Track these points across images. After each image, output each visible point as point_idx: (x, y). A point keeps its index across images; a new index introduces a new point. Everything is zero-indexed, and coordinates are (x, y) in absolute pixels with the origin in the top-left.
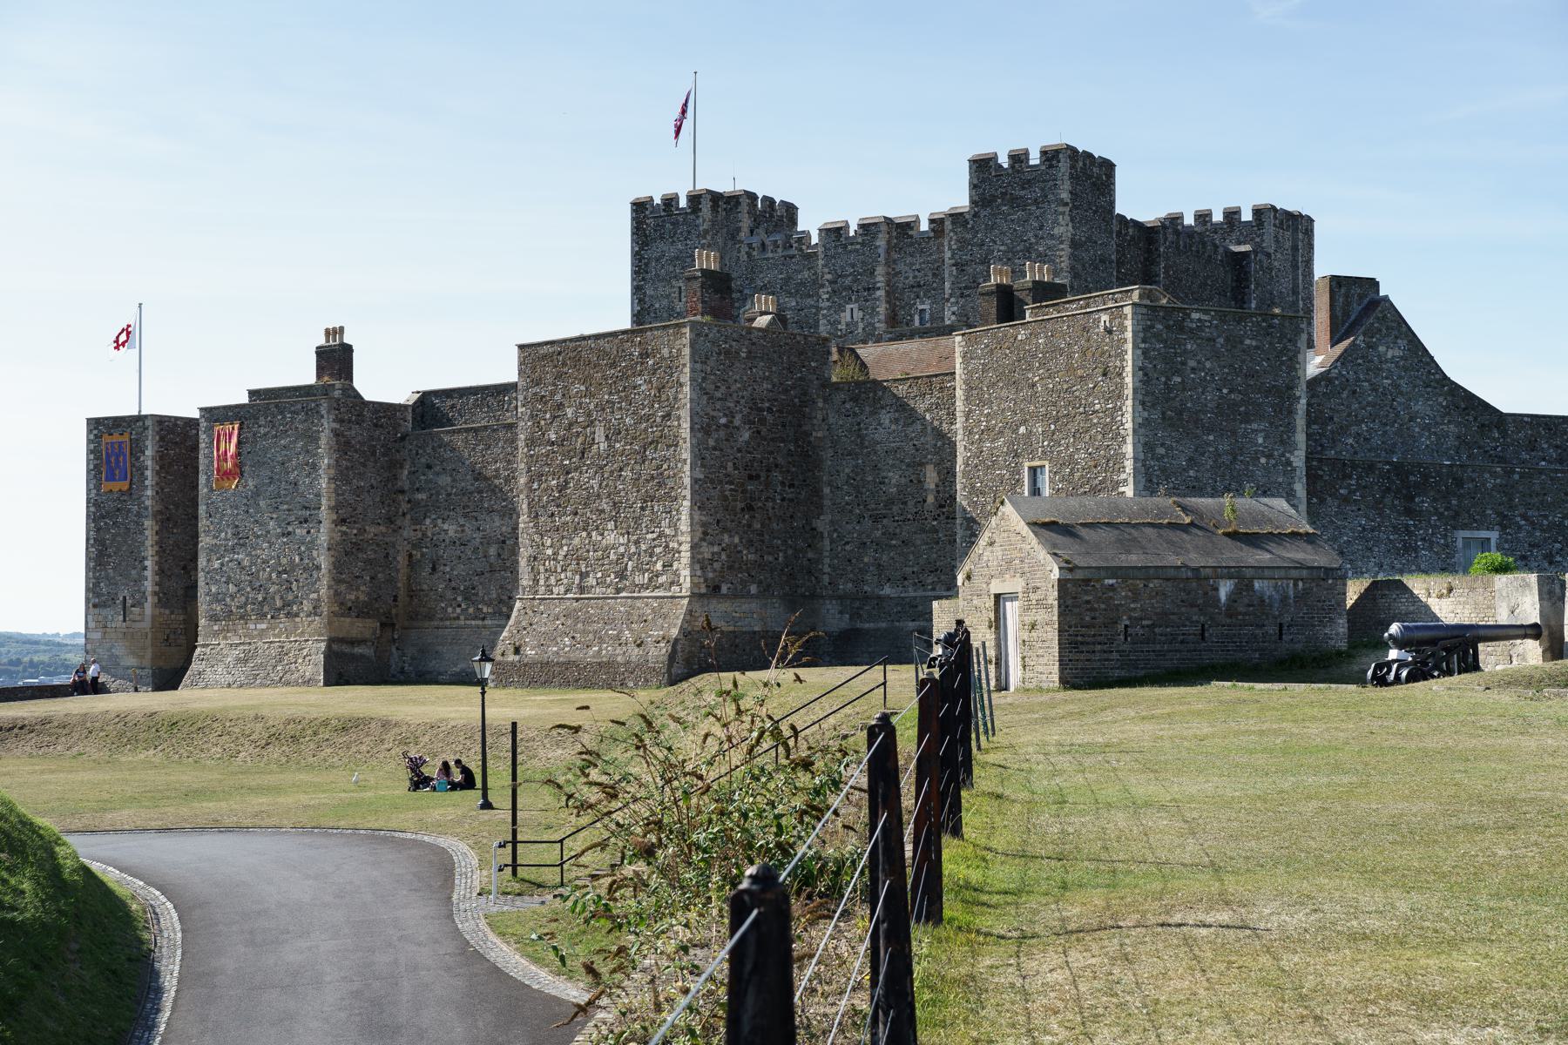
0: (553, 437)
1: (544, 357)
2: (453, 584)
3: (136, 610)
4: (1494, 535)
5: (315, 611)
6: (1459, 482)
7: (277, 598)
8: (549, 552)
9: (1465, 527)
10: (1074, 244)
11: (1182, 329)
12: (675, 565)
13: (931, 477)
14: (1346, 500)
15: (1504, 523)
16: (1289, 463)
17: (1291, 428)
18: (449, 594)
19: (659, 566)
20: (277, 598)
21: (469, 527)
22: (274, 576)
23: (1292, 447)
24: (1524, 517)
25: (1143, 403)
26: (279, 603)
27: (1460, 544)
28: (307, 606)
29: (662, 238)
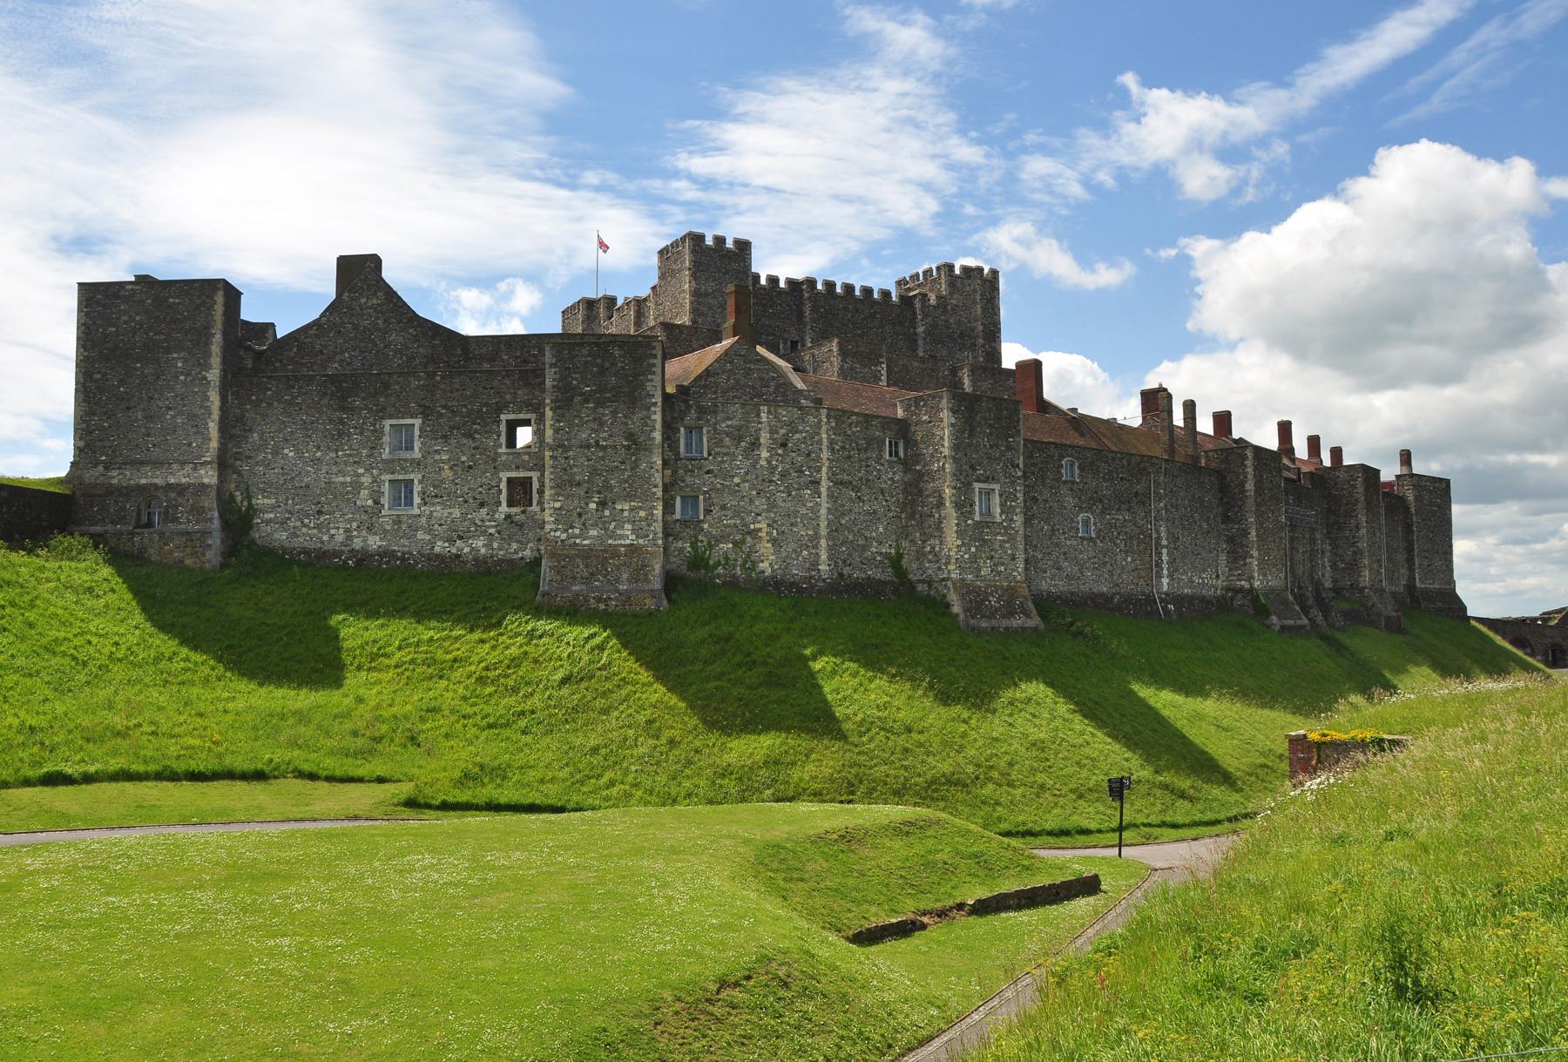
4: (417, 422)
6: (386, 386)
9: (391, 417)
10: (696, 294)
11: (118, 297)
14: (290, 403)
15: (425, 416)
16: (205, 378)
17: (208, 355)
23: (208, 367)
24: (444, 407)
25: (84, 347)
27: (387, 429)
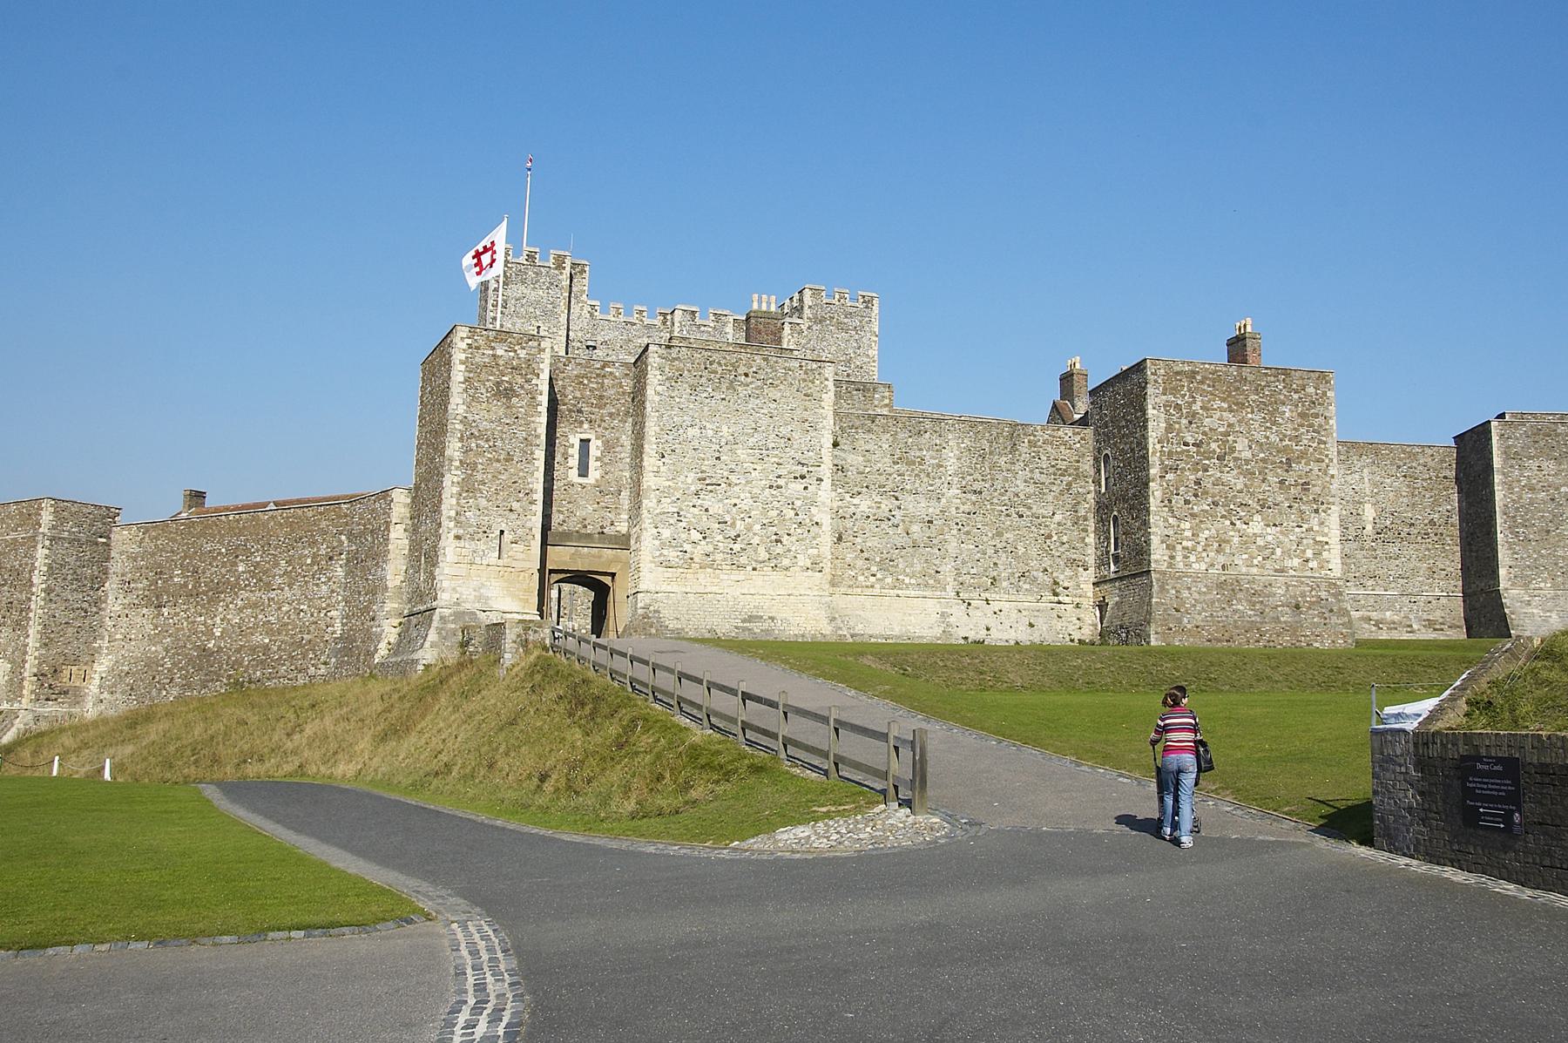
0: (1190, 440)
1: (1178, 373)
2: (865, 555)
3: (519, 547)
5: (816, 566)
7: (761, 550)
8: (1188, 534)
12: (1325, 554)
13: (1369, 512)
18: (860, 563)
19: (1309, 554)
20: (761, 550)
21: (887, 504)
22: (757, 527)
26: (763, 555)
28: (803, 561)
29: (523, 283)
